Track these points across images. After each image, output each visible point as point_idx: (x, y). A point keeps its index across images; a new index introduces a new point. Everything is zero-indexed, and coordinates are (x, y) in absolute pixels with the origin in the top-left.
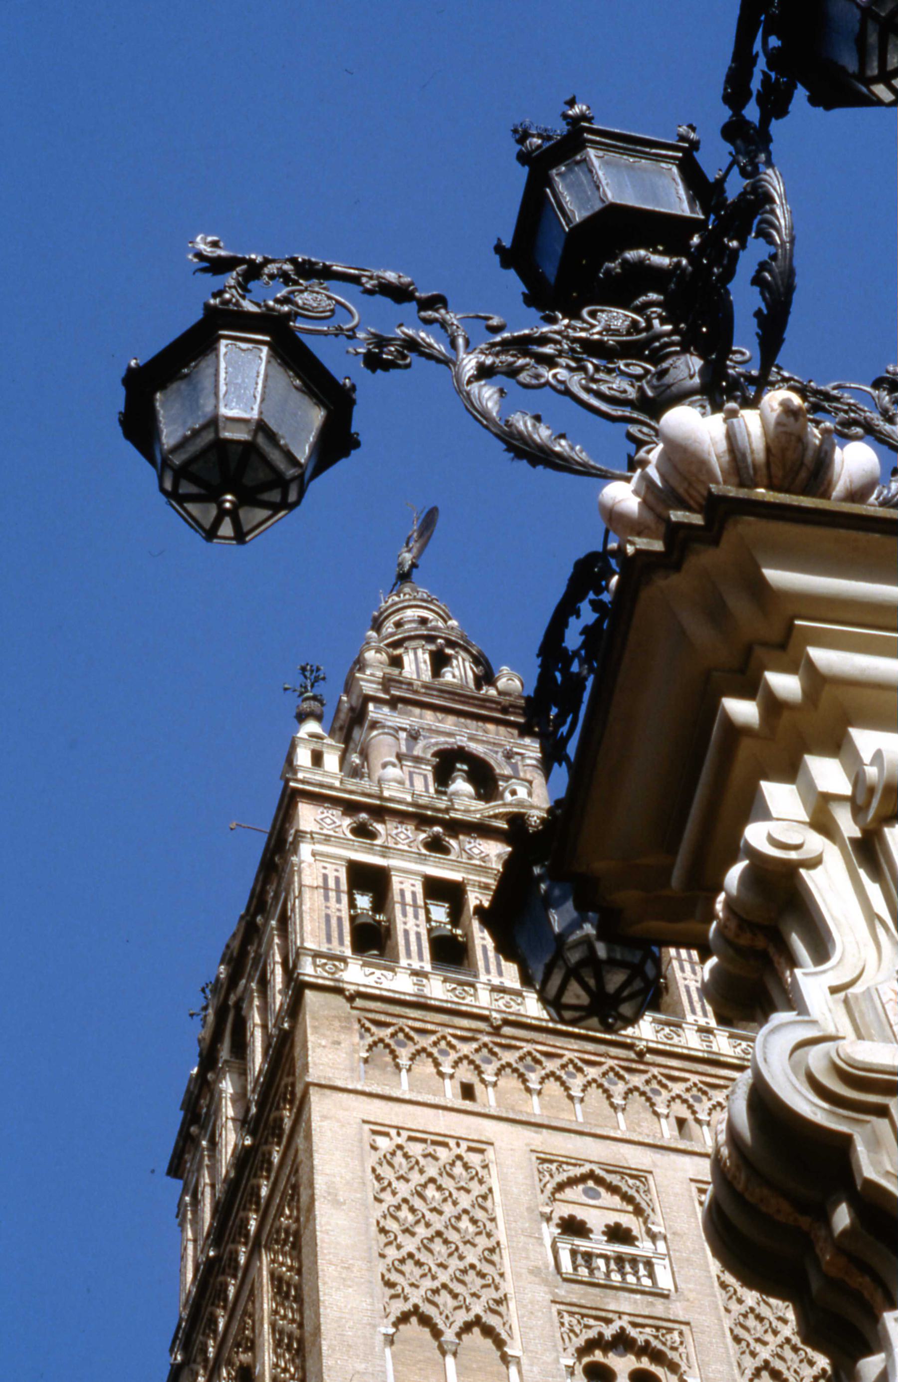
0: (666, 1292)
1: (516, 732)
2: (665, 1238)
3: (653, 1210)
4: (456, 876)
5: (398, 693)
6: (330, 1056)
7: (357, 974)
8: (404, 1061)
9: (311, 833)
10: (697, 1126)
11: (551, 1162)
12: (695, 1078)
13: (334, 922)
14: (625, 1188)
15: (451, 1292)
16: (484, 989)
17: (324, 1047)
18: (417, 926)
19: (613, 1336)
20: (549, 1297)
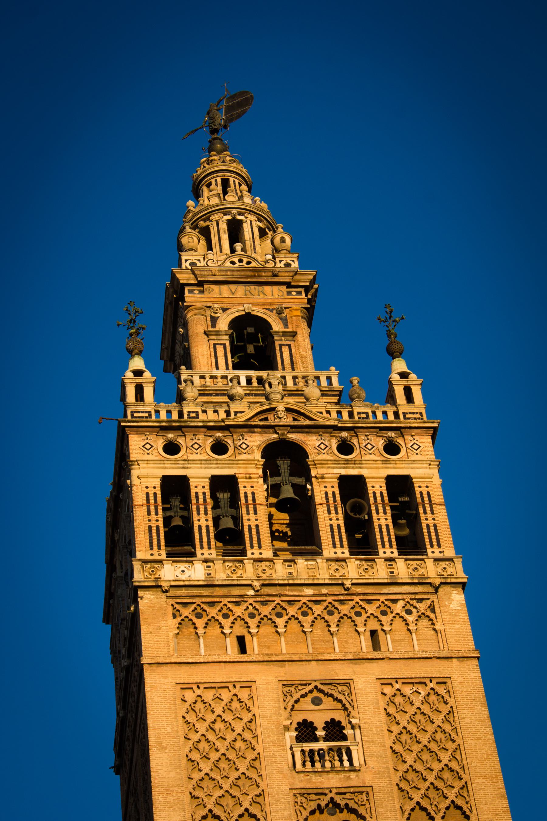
0: (358, 769)
1: (284, 288)
2: (360, 727)
5: (202, 279)
6: (155, 639)
8: (201, 631)
9: (137, 461)
10: (383, 633)
12: (382, 598)
14: (336, 694)
15: (231, 795)
16: (249, 563)
17: (151, 633)
18: (207, 520)
20: (287, 788)
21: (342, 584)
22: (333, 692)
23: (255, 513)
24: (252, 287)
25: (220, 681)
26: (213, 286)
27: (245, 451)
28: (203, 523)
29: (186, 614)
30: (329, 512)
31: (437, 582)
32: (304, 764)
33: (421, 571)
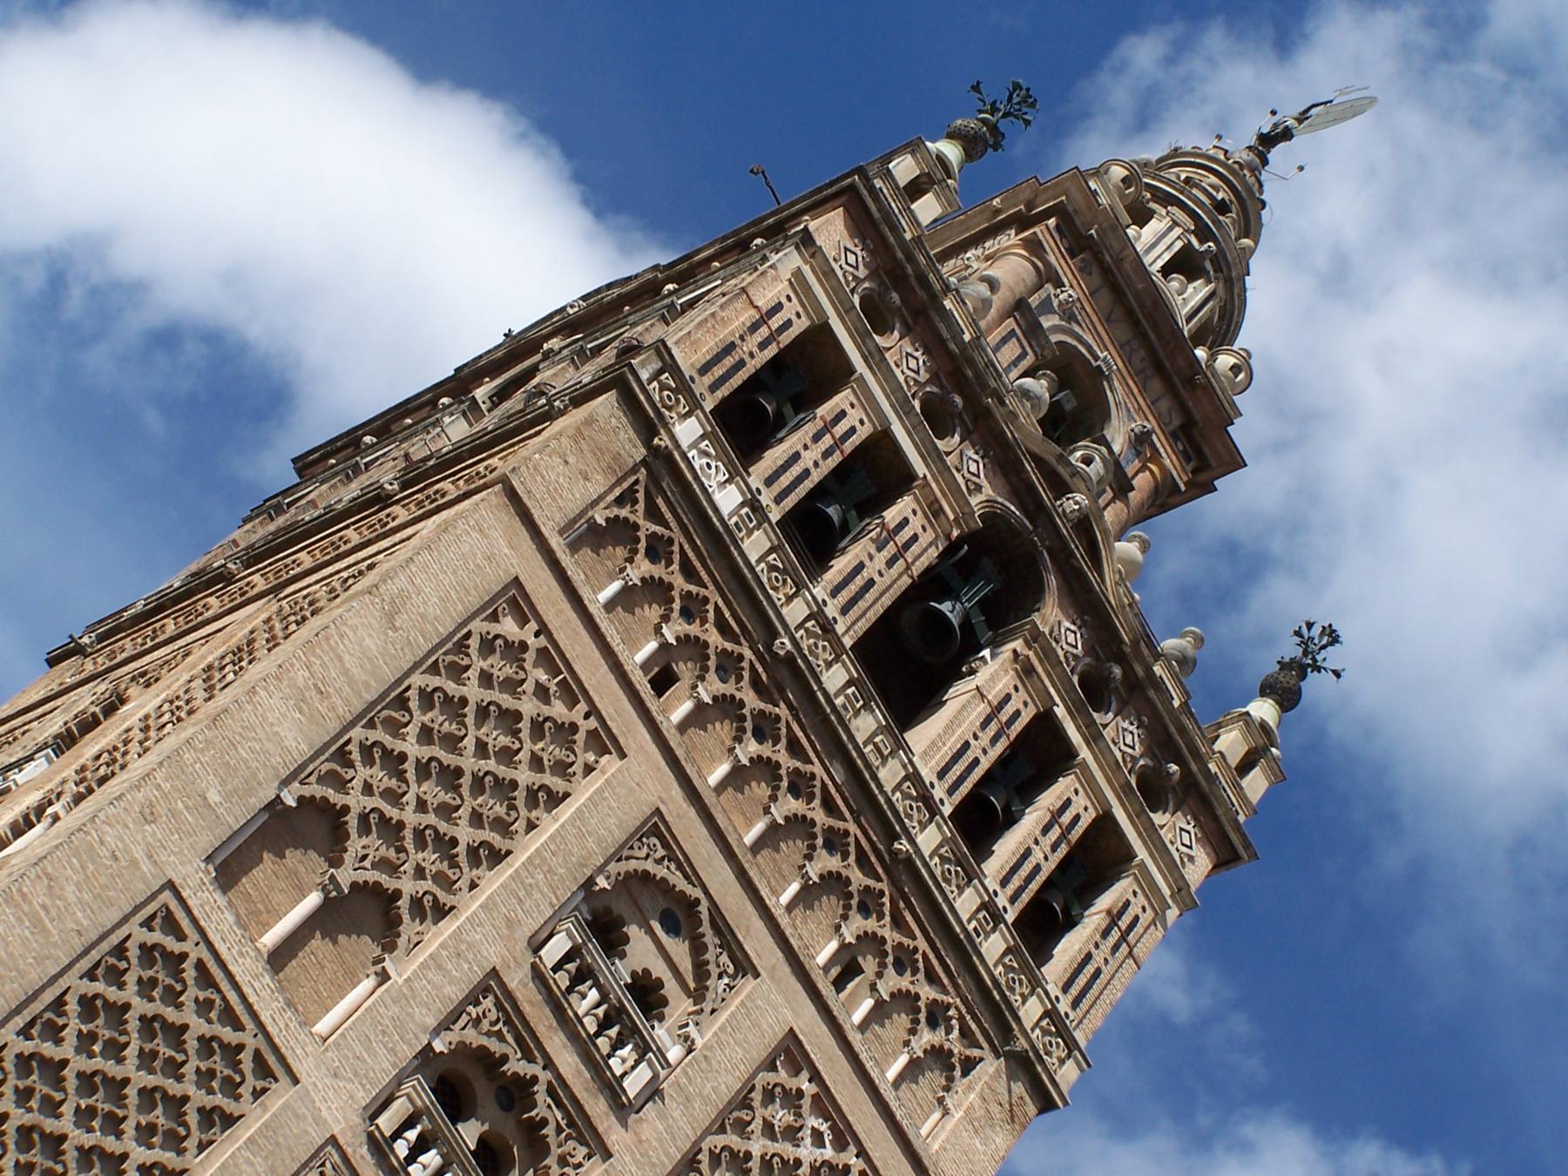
1: (1176, 422)
2: (690, 1051)
3: (713, 1011)
4: (920, 468)
7: (687, 430)
11: (665, 845)
12: (922, 944)
13: (729, 361)
14: (710, 956)
18: (816, 464)
19: (515, 1074)
20: (495, 961)
21: (897, 837)
22: (711, 948)
23: (890, 563)
24: (1142, 353)
25: (583, 677)
26: (1095, 269)
27: (968, 476)
28: (808, 458)
29: (641, 522)
30: (985, 724)
31: (1022, 1043)
32: (557, 967)
33: (1015, 999)
